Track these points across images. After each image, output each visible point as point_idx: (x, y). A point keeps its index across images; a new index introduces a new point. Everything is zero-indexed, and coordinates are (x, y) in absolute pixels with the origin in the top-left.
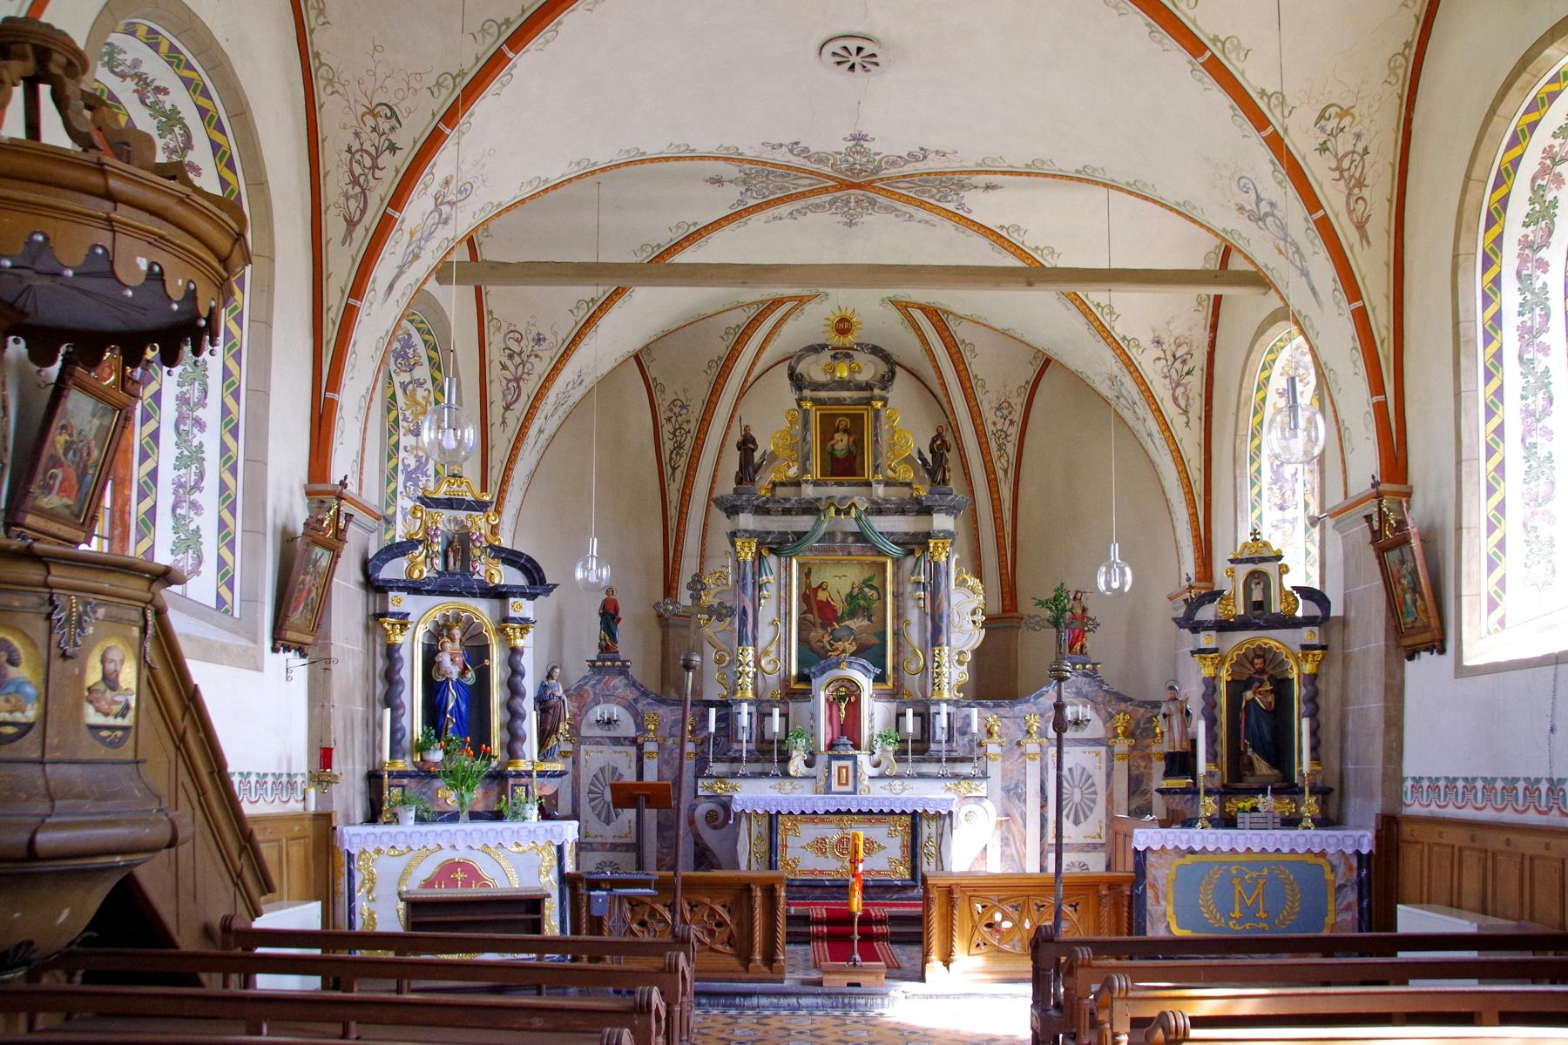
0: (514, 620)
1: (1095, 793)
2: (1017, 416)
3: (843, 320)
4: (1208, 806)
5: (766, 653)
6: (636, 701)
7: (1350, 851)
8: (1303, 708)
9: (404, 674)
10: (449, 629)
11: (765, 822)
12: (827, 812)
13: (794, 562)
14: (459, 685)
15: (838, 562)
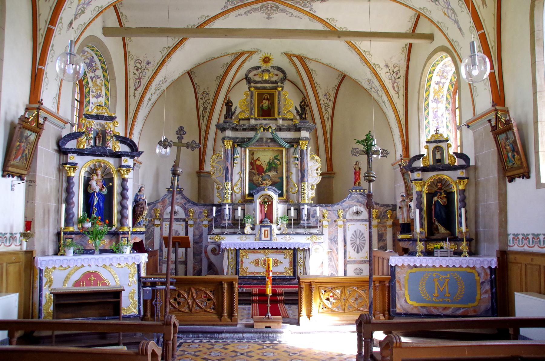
0: (124, 166)
1: (365, 240)
2: (332, 98)
3: (266, 58)
4: (420, 246)
5: (236, 185)
7: (486, 267)
8: (459, 205)
9: (75, 189)
10: (96, 170)
11: (235, 252)
12: (259, 249)
13: (247, 149)
14: (99, 194)
15: (264, 150)
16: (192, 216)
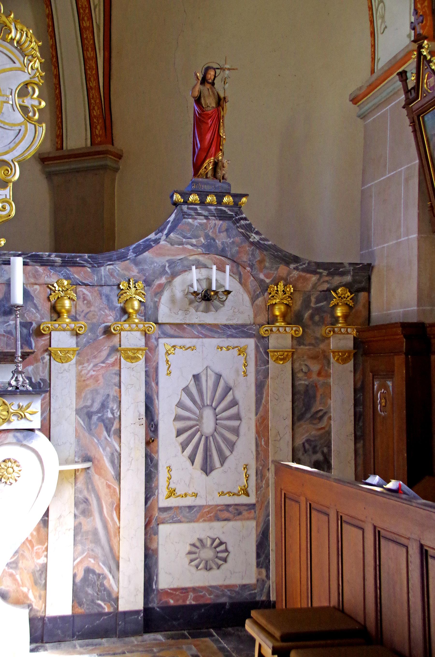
1: (237, 417)
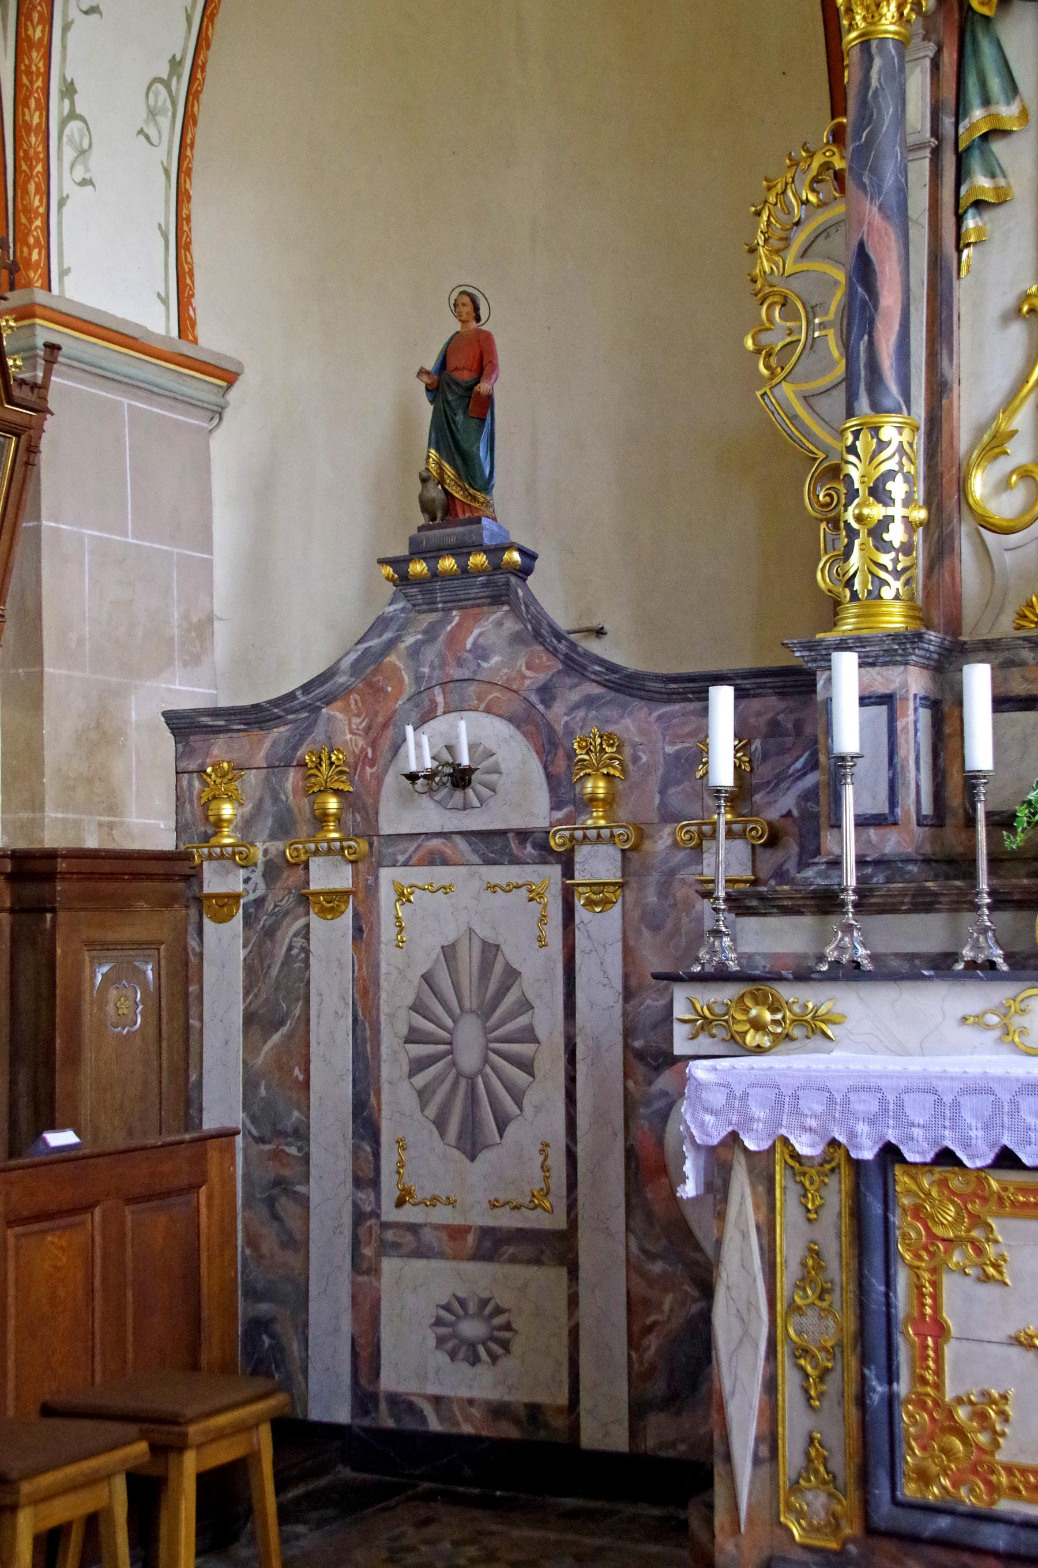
5: (995, 445)
6: (547, 693)
11: (835, 1195)
16: (610, 802)
